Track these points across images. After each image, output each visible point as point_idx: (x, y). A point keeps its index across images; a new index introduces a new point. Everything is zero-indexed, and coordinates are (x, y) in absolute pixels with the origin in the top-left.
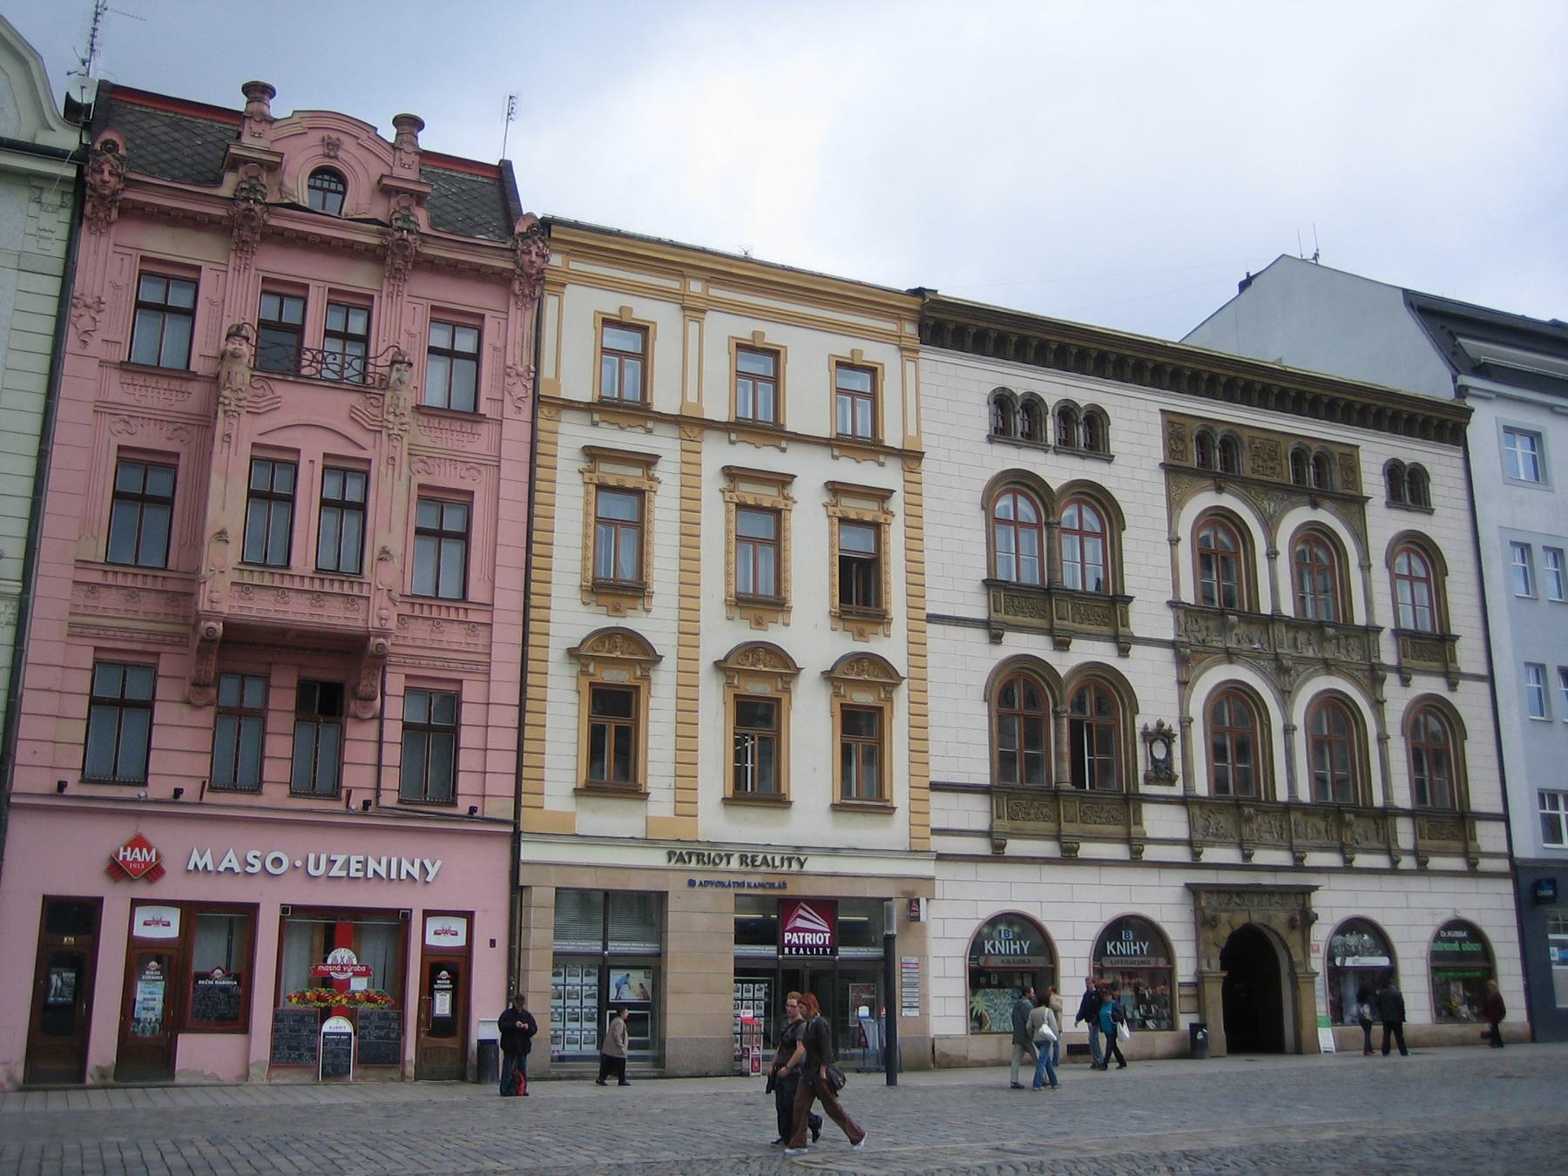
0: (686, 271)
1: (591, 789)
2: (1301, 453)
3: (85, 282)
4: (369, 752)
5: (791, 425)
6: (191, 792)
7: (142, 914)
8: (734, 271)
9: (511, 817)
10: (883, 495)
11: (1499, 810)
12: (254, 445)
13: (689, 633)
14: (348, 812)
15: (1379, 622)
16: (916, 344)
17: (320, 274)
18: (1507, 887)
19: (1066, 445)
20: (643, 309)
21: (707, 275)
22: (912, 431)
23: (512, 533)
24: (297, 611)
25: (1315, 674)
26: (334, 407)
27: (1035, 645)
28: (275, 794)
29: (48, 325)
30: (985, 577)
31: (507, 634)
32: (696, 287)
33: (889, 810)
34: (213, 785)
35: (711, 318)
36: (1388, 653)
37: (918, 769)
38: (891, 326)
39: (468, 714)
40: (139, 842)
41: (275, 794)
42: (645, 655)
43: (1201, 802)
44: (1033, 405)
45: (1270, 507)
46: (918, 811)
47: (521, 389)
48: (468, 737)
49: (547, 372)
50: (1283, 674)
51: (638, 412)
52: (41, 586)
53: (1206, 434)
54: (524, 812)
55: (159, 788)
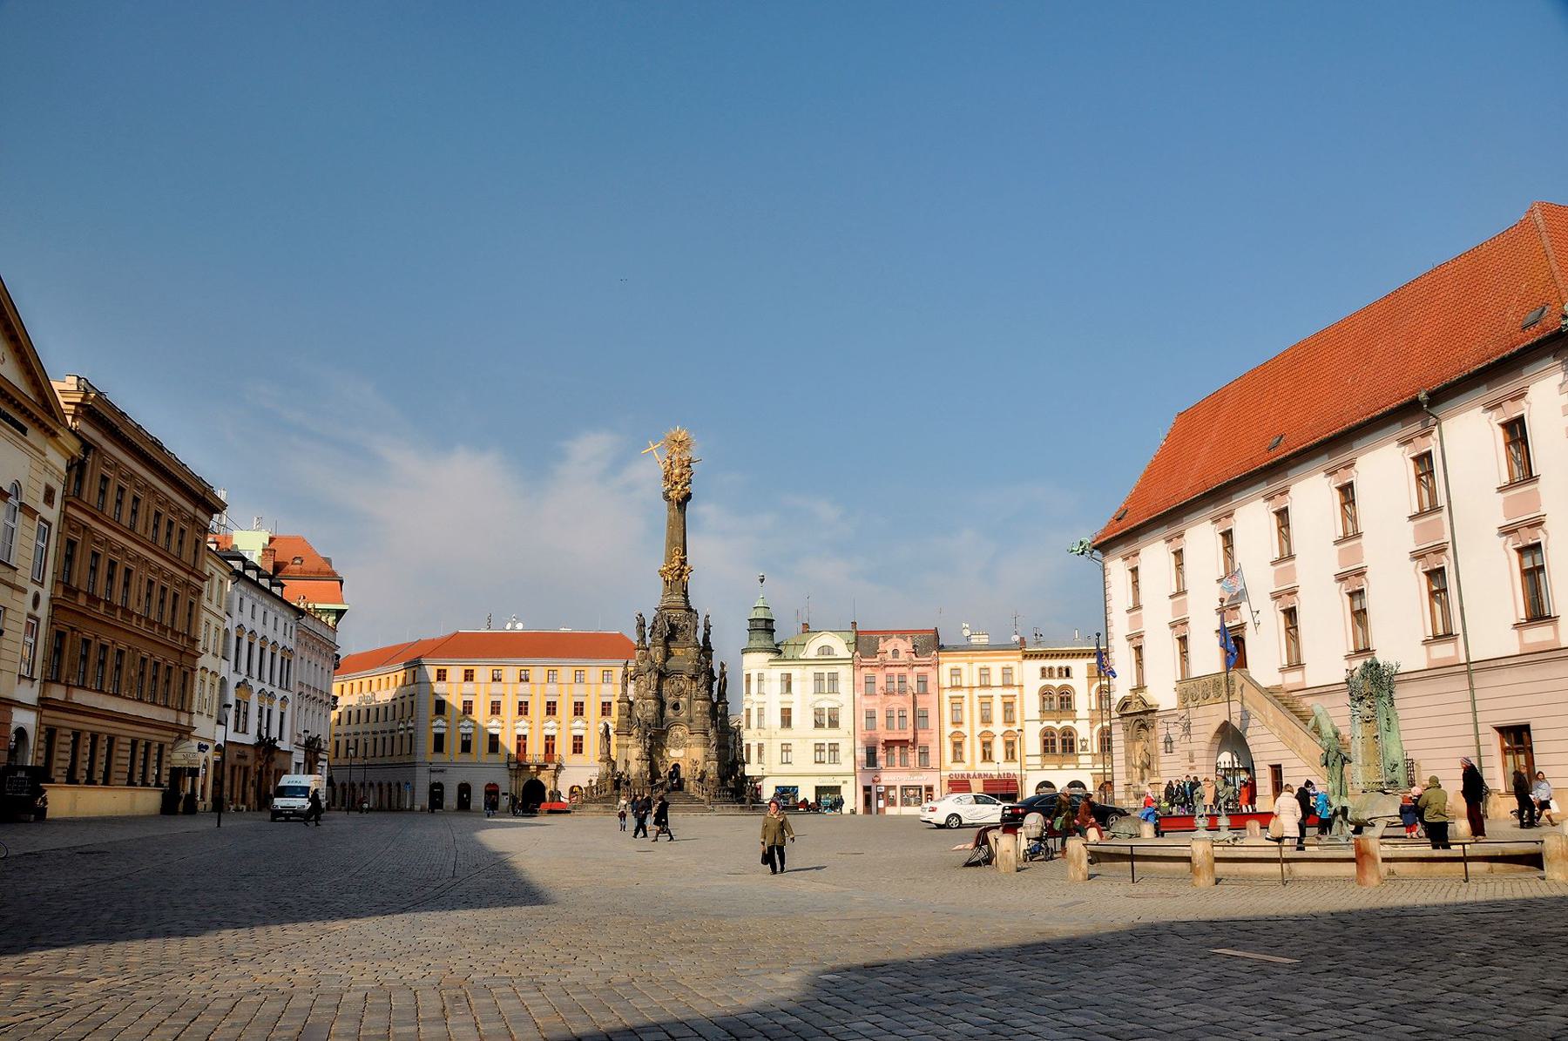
1: (955, 761)
5: (992, 685)
13: (972, 730)
20: (959, 665)
28: (898, 767)
32: (970, 658)
34: (887, 766)
35: (975, 664)
38: (1015, 657)
40: (876, 776)
43: (1095, 755)
44: (1050, 669)
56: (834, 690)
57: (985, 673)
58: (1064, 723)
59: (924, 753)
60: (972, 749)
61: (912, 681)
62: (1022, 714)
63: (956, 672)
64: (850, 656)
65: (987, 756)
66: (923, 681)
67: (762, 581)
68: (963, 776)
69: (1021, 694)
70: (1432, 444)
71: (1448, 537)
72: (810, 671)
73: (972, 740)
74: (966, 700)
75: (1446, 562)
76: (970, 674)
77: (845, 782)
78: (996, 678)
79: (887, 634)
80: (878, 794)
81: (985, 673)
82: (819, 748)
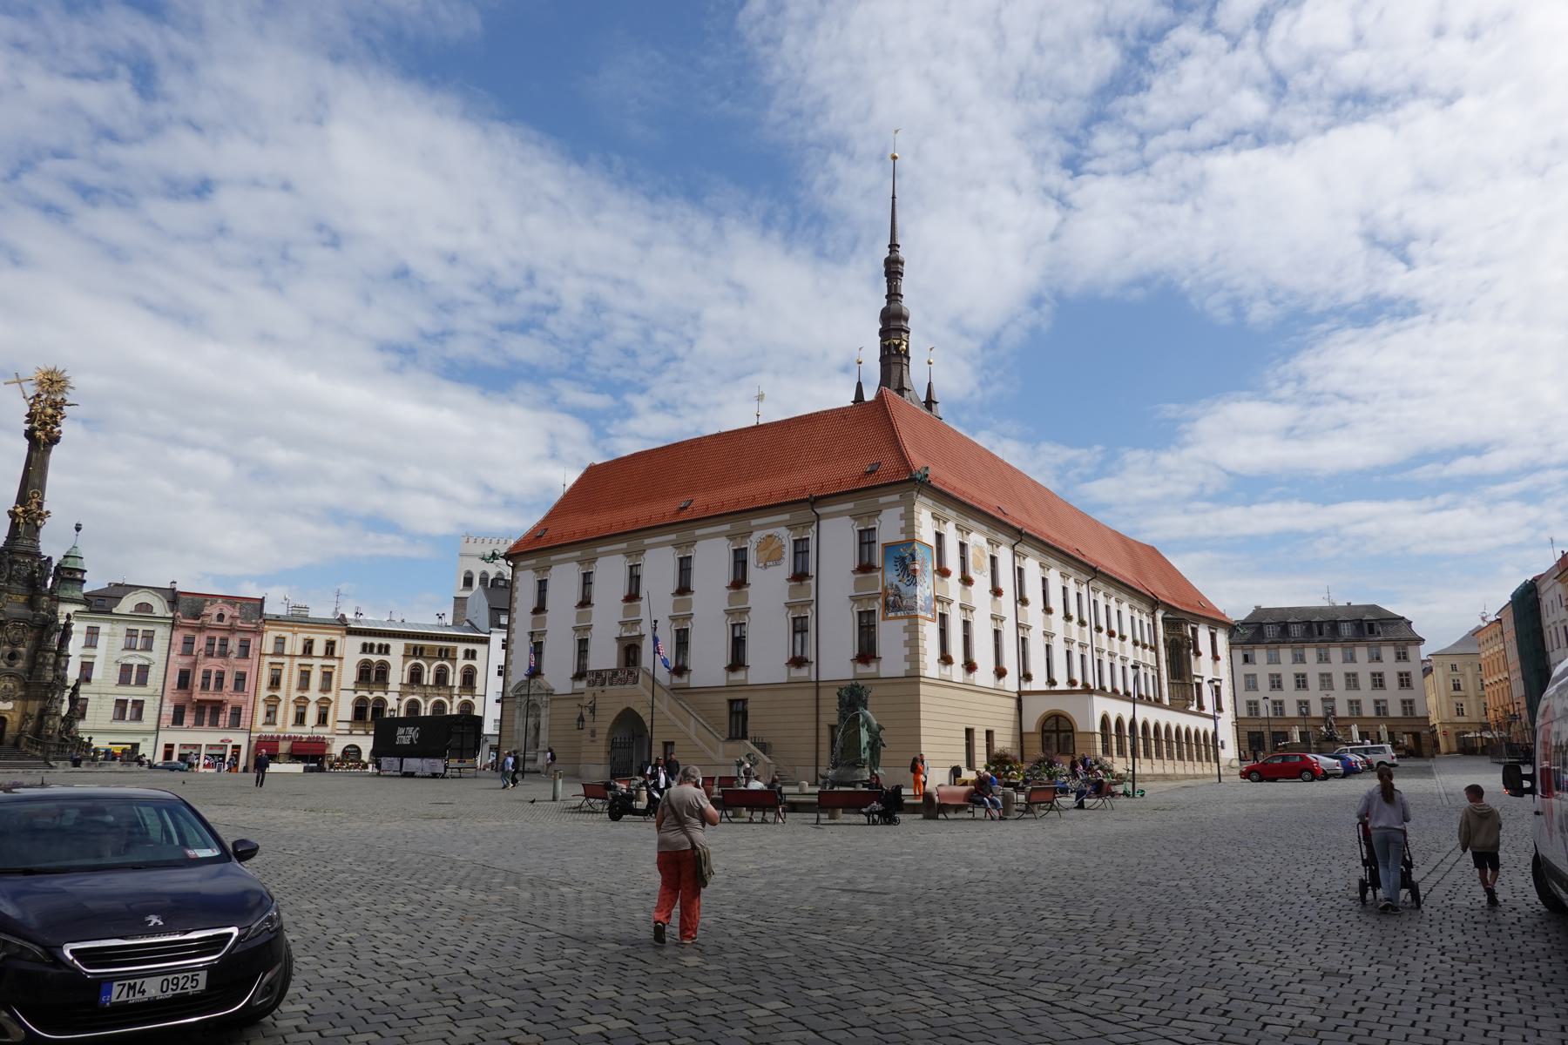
3: (174, 641)
4: (223, 719)
6: (191, 726)
10: (333, 667)
13: (288, 695)
17: (218, 635)
19: (380, 652)
20: (284, 634)
23: (254, 679)
24: (210, 697)
26: (218, 661)
27: (365, 694)
32: (296, 629)
33: (327, 726)
36: (456, 691)
38: (340, 632)
39: (243, 711)
42: (278, 700)
44: (372, 645)
45: (430, 662)
46: (334, 725)
47: (258, 652)
48: (243, 715)
50: (426, 697)
51: (282, 654)
52: (165, 693)
55: (185, 726)
58: (376, 694)
59: (237, 712)
60: (286, 713)
61: (234, 643)
63: (280, 641)
64: (171, 615)
65: (300, 719)
67: (78, 528)
68: (272, 737)
70: (811, 534)
71: (813, 597)
72: (121, 629)
75: (810, 613)
76: (294, 644)
77: (145, 740)
78: (319, 648)
79: (214, 598)
82: (121, 704)
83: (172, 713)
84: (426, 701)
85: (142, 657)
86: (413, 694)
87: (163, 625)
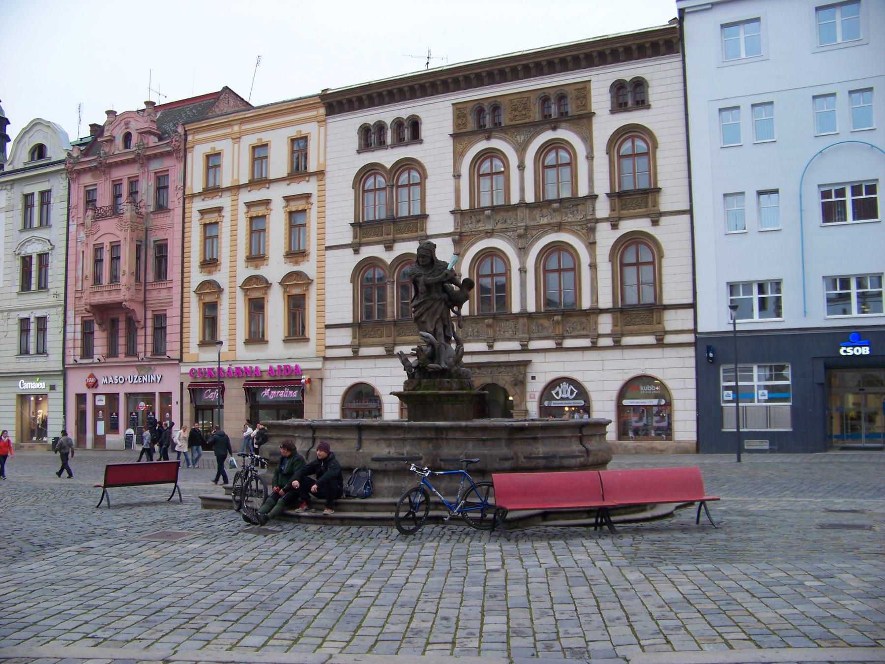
0: (232, 123)
2: (544, 98)
6: (103, 360)
7: (98, 397)
8: (247, 116)
9: (179, 357)
10: (307, 196)
11: (690, 301)
12: (94, 245)
13: (233, 277)
14: (139, 361)
15: (596, 192)
16: (323, 118)
17: (123, 174)
18: (691, 351)
19: (400, 141)
21: (239, 122)
22: (322, 161)
25: (545, 233)
28: (122, 357)
29: (66, 218)
30: (353, 221)
31: (177, 290)
32: (236, 128)
33: (307, 340)
37: (321, 320)
38: (313, 113)
41: (122, 357)
44: (380, 127)
45: (521, 138)
46: (321, 338)
49: (188, 184)
53: (479, 108)
54: (184, 355)
55: (96, 357)
56: (45, 223)
57: (259, 153)
62: (321, 236)
63: (213, 161)
66: (161, 188)
69: (322, 191)
73: (233, 297)
74: (227, 213)
77: (53, 388)
80: (96, 409)
81: (259, 153)
83: (79, 336)
84: (523, 251)
85: (39, 239)
86: (490, 234)
87: (59, 177)
